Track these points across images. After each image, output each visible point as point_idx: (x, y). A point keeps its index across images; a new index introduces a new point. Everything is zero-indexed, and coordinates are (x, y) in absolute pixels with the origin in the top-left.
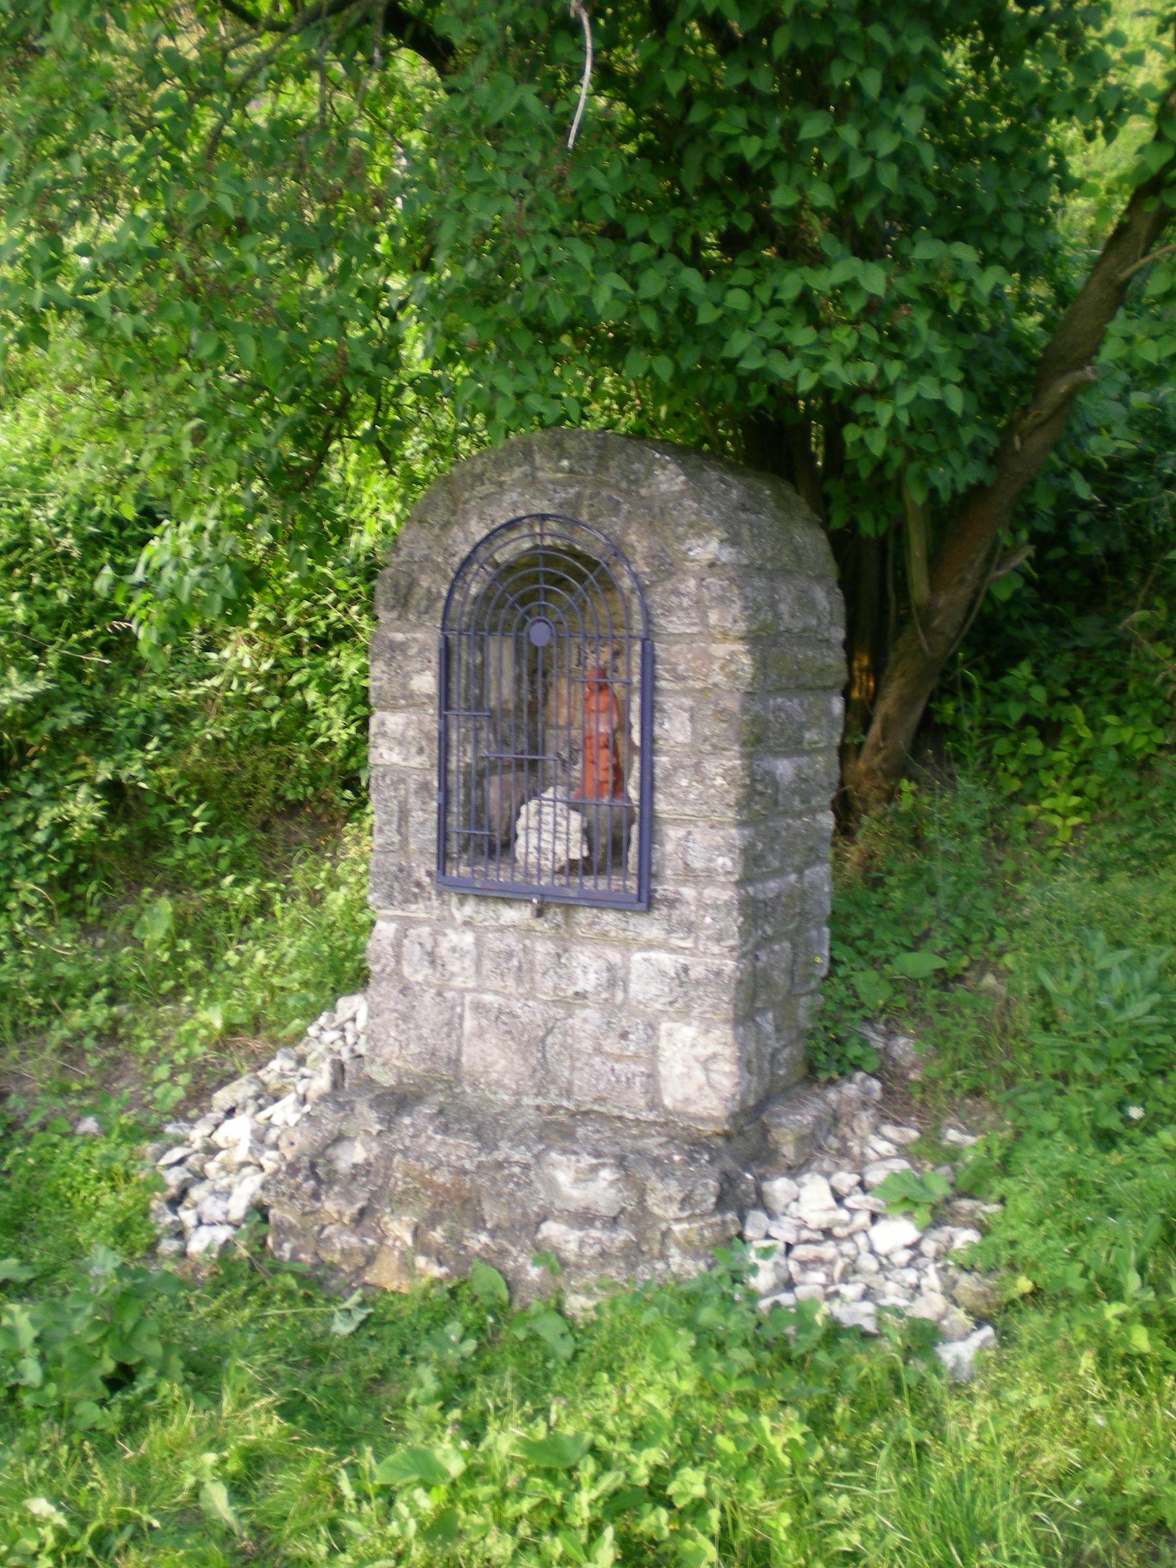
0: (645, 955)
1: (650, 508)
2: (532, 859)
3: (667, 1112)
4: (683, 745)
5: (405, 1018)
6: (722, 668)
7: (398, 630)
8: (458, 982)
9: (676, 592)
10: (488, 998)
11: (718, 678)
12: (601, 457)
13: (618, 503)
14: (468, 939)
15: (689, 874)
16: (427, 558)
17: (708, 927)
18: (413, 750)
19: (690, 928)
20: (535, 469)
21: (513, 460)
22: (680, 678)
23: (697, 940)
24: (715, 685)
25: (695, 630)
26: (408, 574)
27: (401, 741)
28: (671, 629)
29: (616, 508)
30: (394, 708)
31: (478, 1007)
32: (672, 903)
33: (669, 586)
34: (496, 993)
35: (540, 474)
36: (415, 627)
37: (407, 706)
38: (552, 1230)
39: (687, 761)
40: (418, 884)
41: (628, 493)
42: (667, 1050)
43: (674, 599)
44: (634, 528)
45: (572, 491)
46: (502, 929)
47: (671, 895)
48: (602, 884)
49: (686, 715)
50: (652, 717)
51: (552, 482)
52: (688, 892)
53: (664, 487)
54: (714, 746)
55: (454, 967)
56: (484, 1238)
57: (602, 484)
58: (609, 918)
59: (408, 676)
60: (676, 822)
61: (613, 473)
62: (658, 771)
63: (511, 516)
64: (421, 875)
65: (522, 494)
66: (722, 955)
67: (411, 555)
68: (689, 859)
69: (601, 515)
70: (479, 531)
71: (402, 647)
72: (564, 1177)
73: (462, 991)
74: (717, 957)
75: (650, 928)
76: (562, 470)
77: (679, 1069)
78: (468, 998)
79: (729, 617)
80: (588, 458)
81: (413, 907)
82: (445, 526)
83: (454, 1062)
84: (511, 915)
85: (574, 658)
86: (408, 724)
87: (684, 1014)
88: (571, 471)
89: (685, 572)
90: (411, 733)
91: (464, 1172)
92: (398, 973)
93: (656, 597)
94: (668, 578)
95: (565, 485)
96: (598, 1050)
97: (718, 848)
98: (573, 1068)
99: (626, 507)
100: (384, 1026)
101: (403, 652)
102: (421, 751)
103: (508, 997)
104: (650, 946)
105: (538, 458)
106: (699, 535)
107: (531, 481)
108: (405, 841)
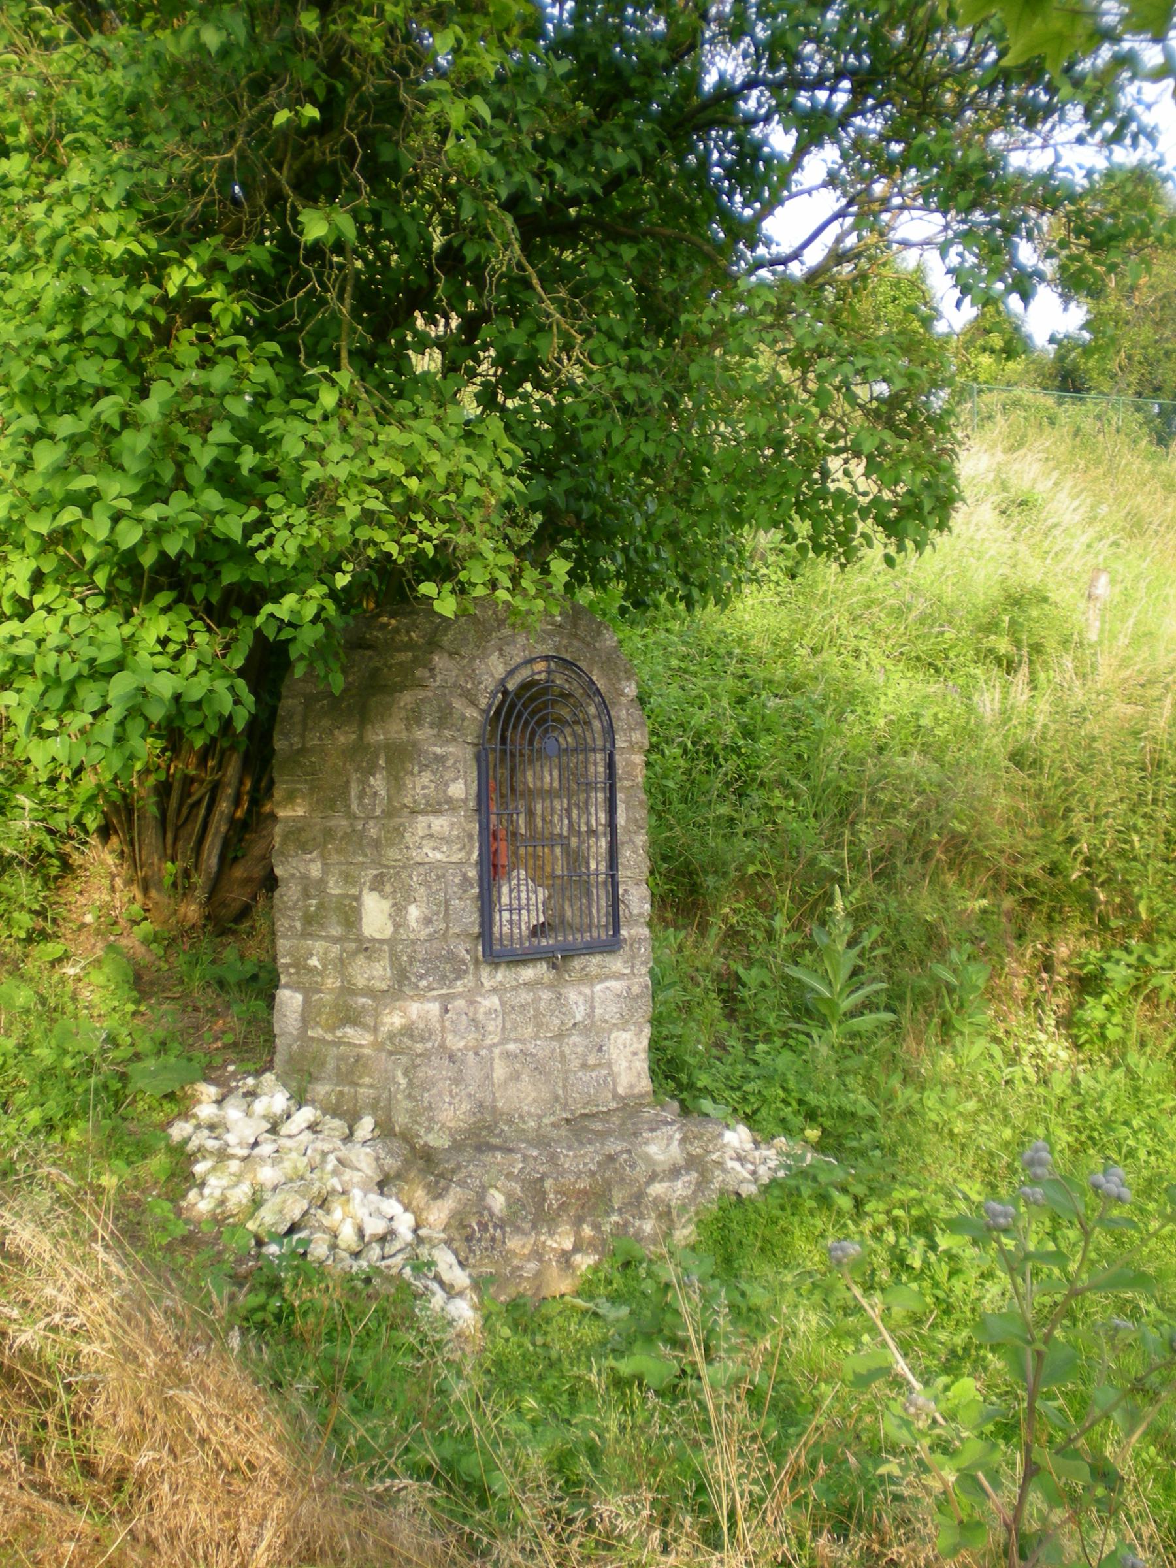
2: (506, 930)
3: (622, 1098)
5: (457, 1081)
8: (488, 1042)
10: (511, 1047)
14: (495, 1000)
27: (446, 840)
30: (437, 812)
31: (507, 1055)
34: (516, 1041)
36: (447, 742)
38: (657, 1189)
40: (463, 962)
48: (544, 942)
55: (491, 1027)
56: (615, 1218)
58: (596, 960)
59: (447, 785)
71: (440, 759)
72: (652, 1149)
73: (490, 1048)
75: (616, 964)
77: (624, 1064)
78: (497, 1051)
82: (472, 659)
83: (494, 1108)
84: (528, 973)
86: (452, 824)
91: (593, 1174)
92: (442, 1045)
95: (551, 635)
96: (584, 1066)
98: (564, 1087)
100: (440, 1094)
103: (523, 1042)
104: (607, 978)
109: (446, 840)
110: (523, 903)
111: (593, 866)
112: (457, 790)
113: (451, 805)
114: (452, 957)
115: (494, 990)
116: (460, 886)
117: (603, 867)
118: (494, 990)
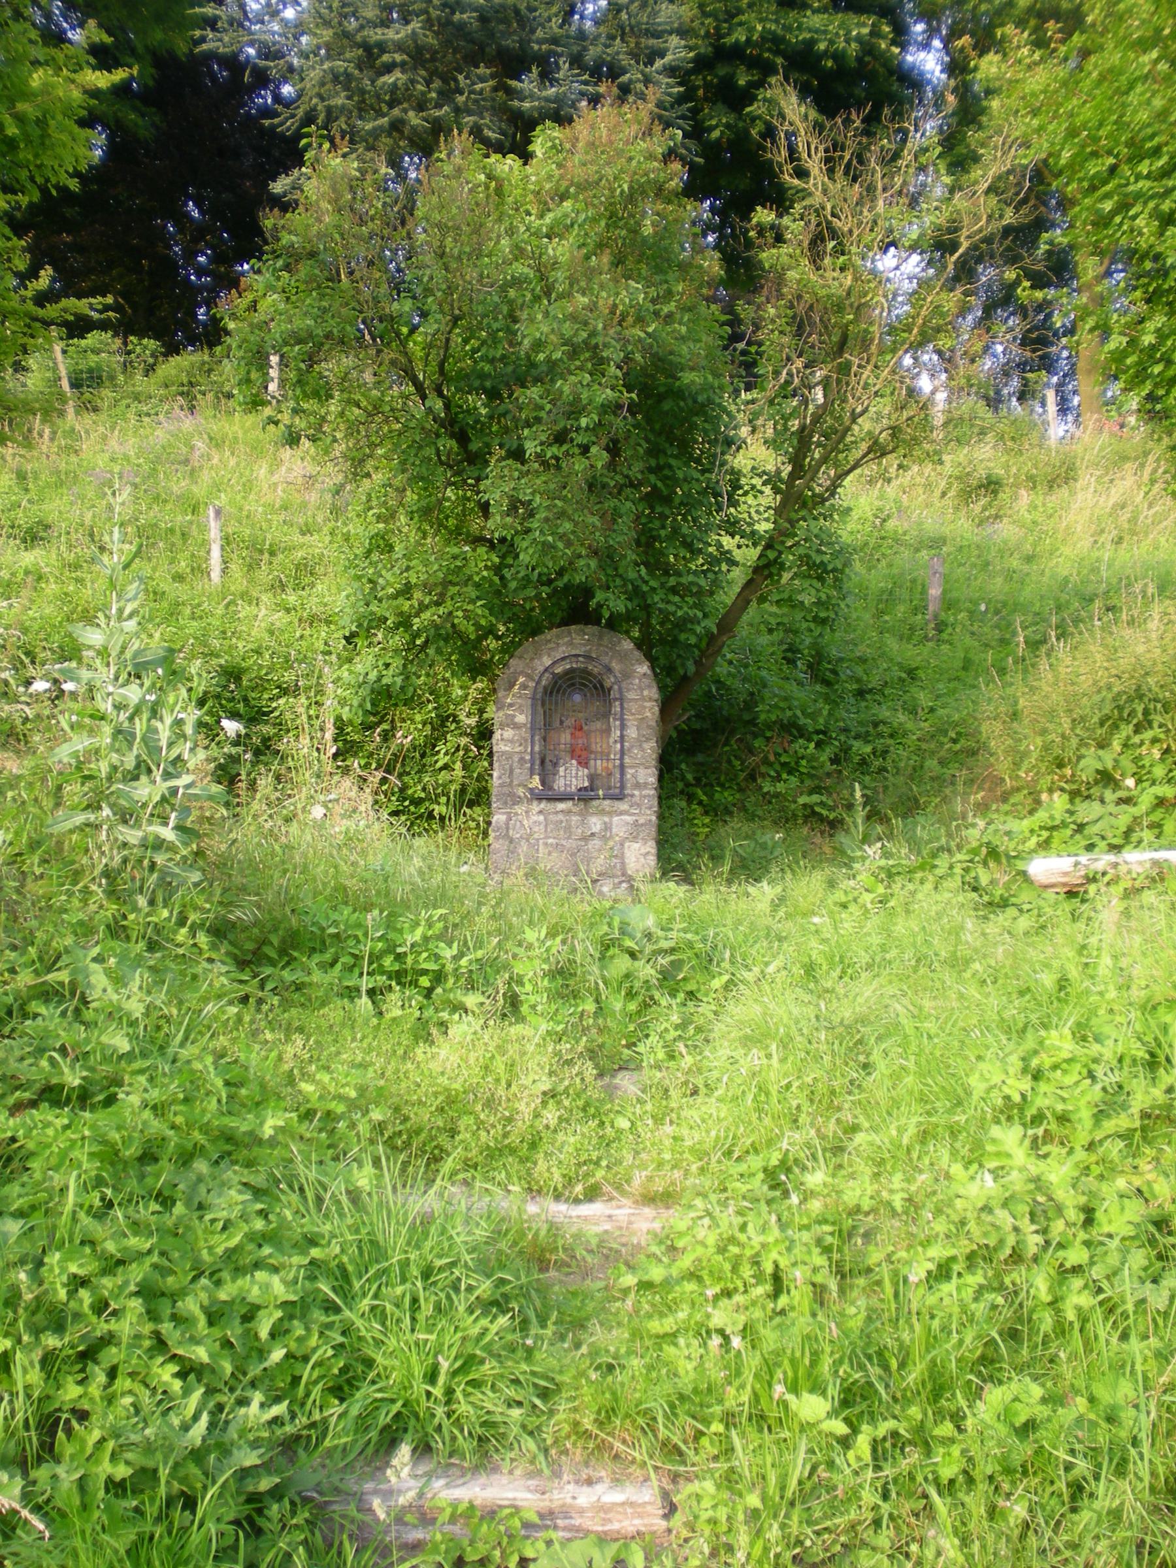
15: (637, 786)
27: (511, 741)
42: (627, 853)
61: (605, 641)
70: (547, 661)
74: (648, 814)
75: (623, 806)
79: (653, 692)
84: (561, 806)
87: (635, 838)
107: (570, 643)
109: (511, 741)
112: (521, 718)
113: (516, 726)
114: (512, 795)
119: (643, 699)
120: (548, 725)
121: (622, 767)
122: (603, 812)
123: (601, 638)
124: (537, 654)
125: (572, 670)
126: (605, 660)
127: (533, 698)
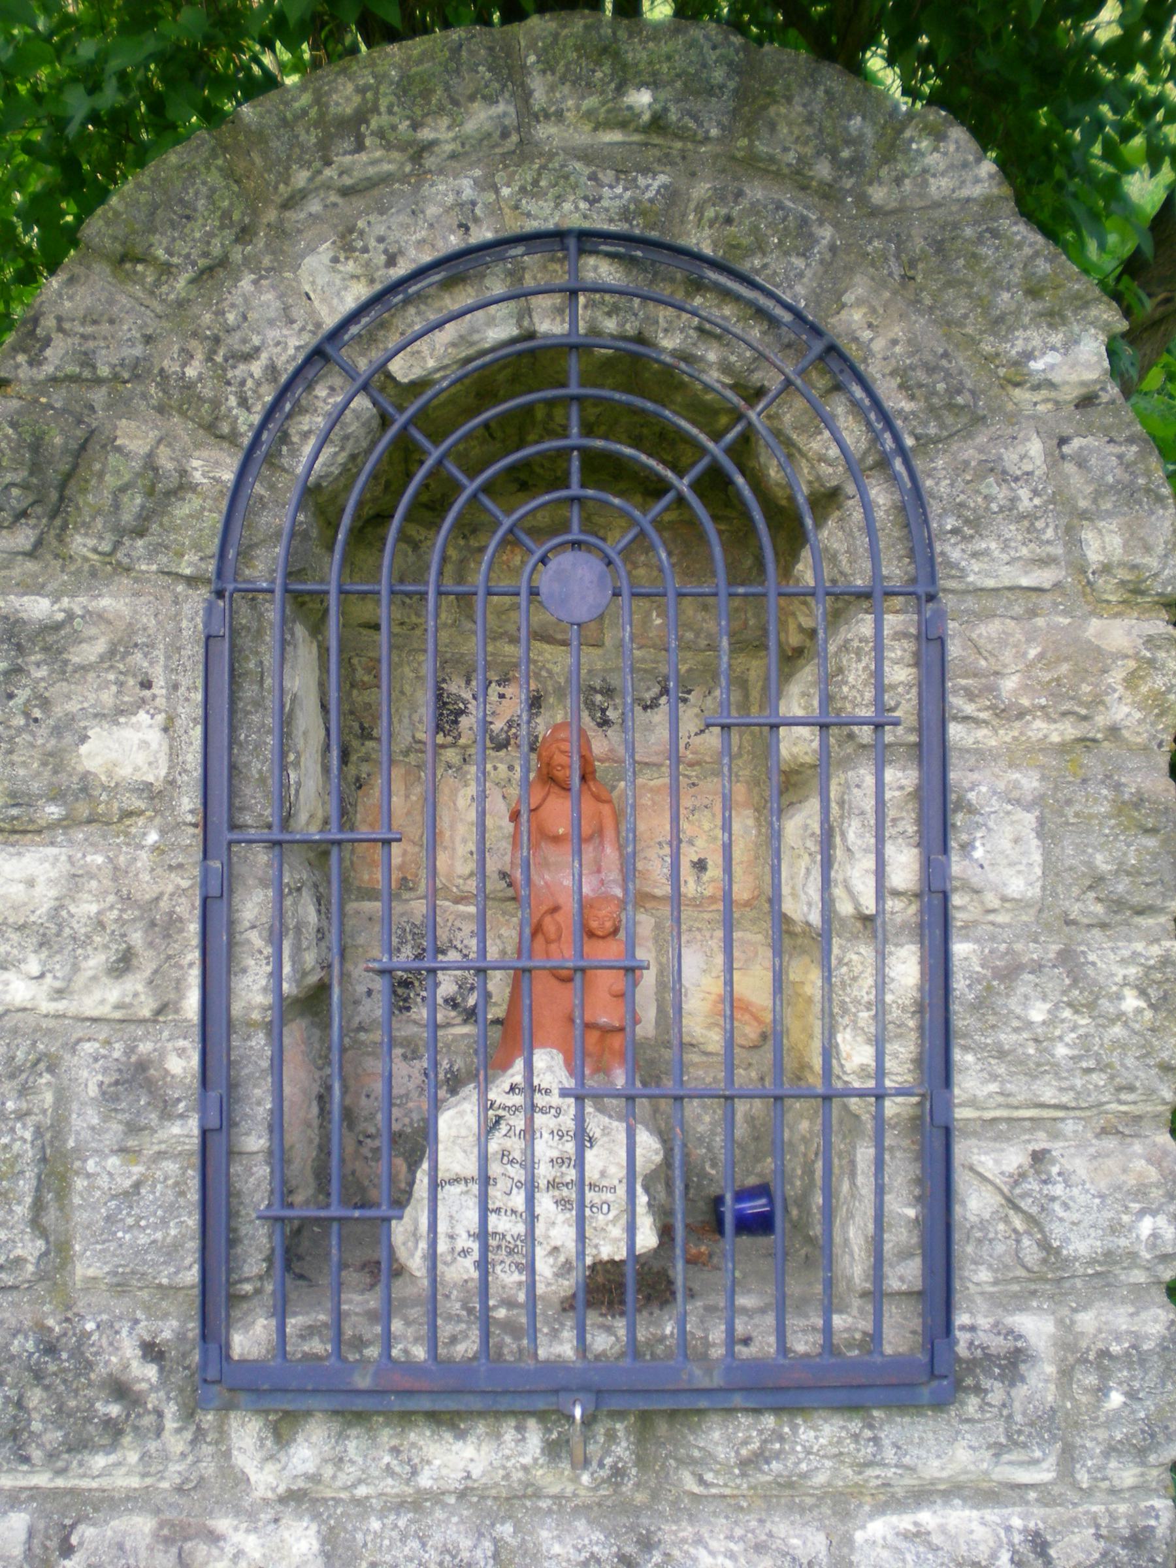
0: (905, 1522)
1: (900, 241)
4: (1019, 904)
6: (1131, 682)
7: (33, 588)
9: (992, 468)
11: (1122, 711)
12: (741, 95)
13: (804, 221)
15: (1050, 1276)
16: (138, 371)
17: (1114, 1419)
18: (96, 961)
19: (1057, 1428)
20: (528, 115)
21: (463, 86)
22: (1008, 714)
23: (1068, 1458)
24: (1114, 731)
25: (1044, 577)
26: (78, 415)
28: (976, 574)
29: (800, 236)
32: (1013, 1363)
33: (969, 453)
35: (544, 131)
37: (68, 823)
39: (1031, 952)
40: (120, 1390)
41: (829, 194)
43: (990, 485)
44: (859, 288)
45: (654, 184)
46: (418, 1503)
47: (998, 1344)
49: (1029, 819)
50: (945, 828)
51: (586, 156)
52: (1036, 1327)
53: (940, 186)
54: (1117, 905)
57: (753, 164)
59: (71, 730)
60: (996, 1130)
61: (787, 135)
62: (959, 984)
63: (455, 242)
64: (125, 1355)
65: (487, 184)
66: (1141, 1489)
67: (87, 360)
68: (1056, 1232)
69: (760, 247)
70: (332, 288)
71: (52, 639)
75: (943, 1448)
76: (624, 121)
80: (711, 91)
81: (100, 1461)
82: (213, 272)
84: (455, 1459)
85: (425, 711)
86: (75, 880)
88: (657, 123)
89: (1013, 419)
90: (86, 908)
93: (939, 481)
94: (967, 433)
95: (625, 169)
97: (1140, 1192)
99: (826, 233)
101: (55, 654)
102: (124, 964)
104: (922, 1496)
105: (539, 86)
106: (1053, 318)
107: (515, 148)
108: (59, 1253)
110: (525, 1184)
111: (855, 1055)
112: (136, 749)
113: (88, 809)
115: (296, 1498)
116: (109, 1097)
117: (901, 1062)
118: (296, 1498)
119: (1085, 589)
120: (354, 736)
121: (937, 1143)
122: (788, 1494)
123: (750, 104)
124: (257, 230)
125: (528, 361)
126: (796, 280)
127: (224, 583)
